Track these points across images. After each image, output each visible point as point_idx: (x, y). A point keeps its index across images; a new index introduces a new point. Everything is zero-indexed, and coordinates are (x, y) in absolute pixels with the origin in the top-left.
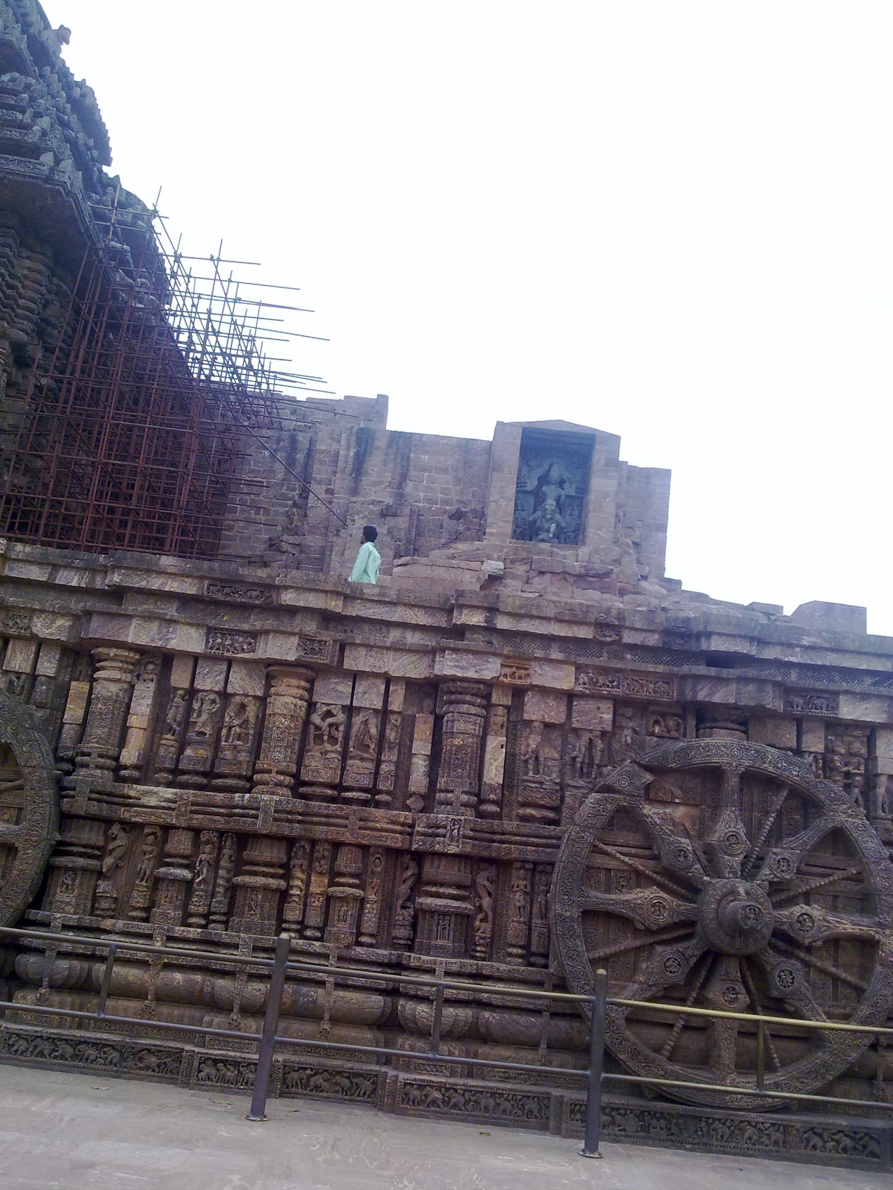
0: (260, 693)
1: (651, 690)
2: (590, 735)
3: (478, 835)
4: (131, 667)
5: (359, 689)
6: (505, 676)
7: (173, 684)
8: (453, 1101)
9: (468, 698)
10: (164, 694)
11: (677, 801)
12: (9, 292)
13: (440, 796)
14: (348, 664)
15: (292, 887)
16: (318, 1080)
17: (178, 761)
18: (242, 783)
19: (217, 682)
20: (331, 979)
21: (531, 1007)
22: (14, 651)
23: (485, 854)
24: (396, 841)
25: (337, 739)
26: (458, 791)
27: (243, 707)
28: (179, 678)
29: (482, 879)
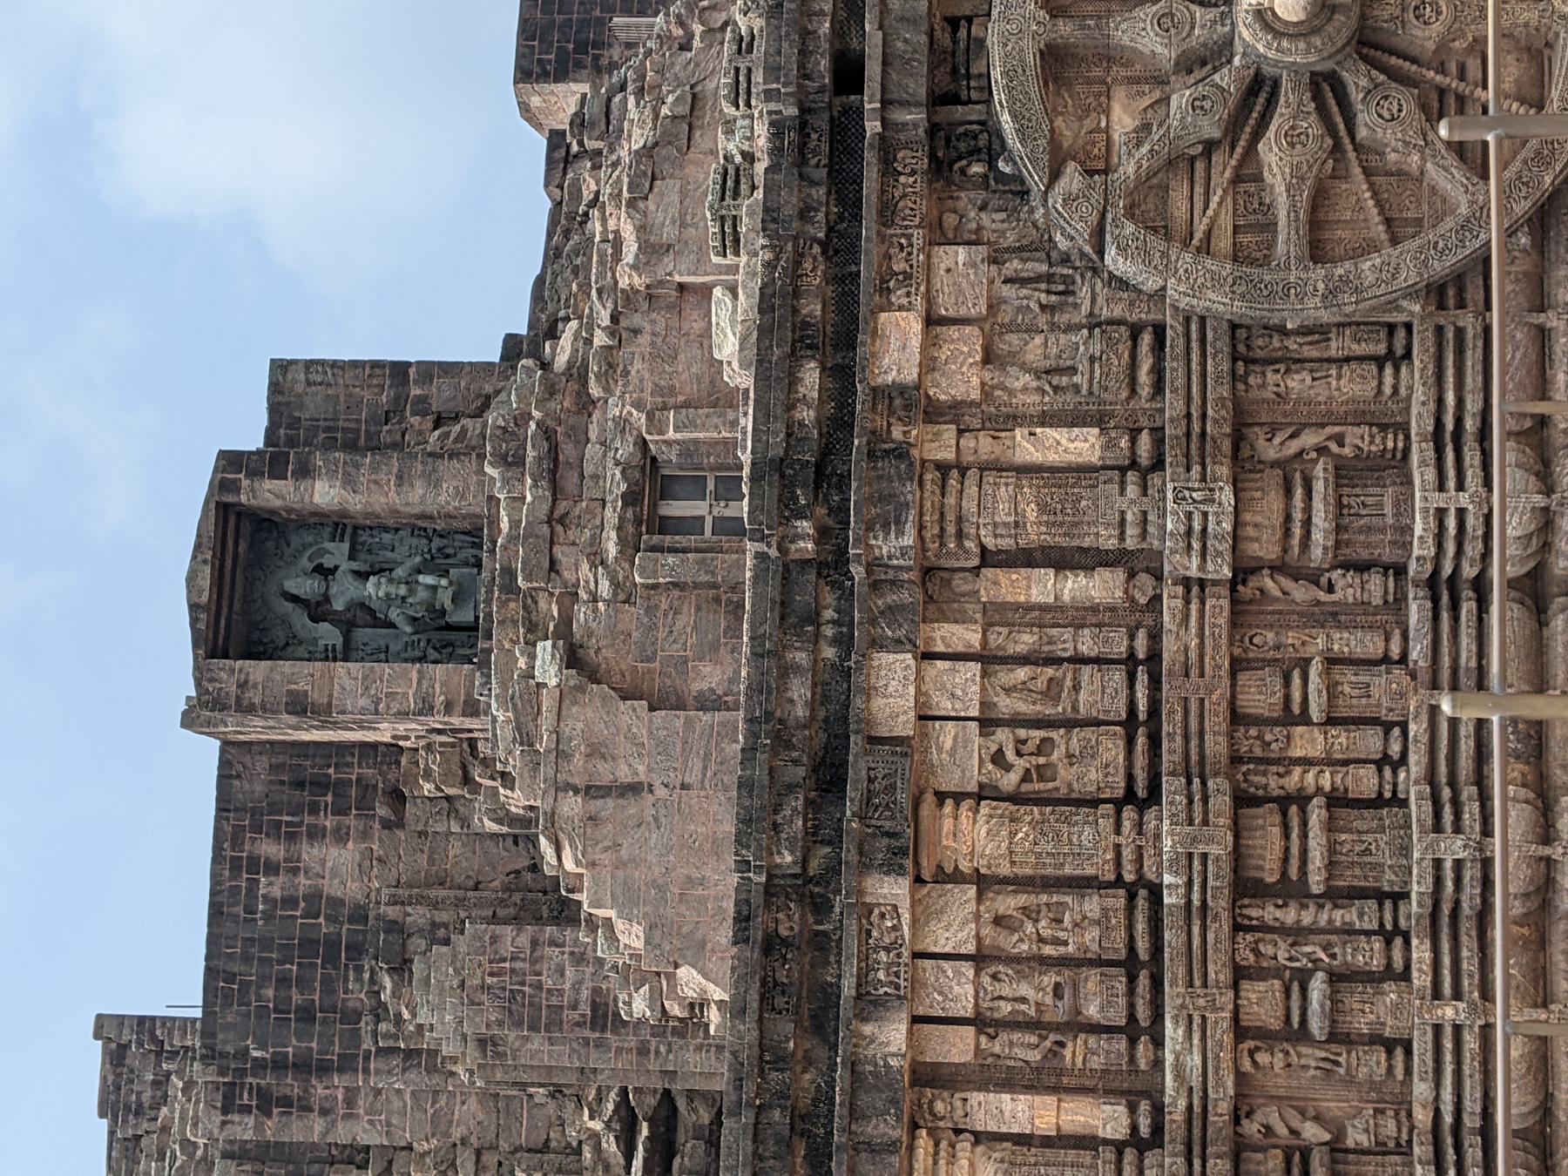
0: (972, 891)
1: (911, 180)
2: (998, 283)
4: (944, 1144)
5: (946, 706)
7: (968, 1057)
11: (1103, 124)
13: (1130, 544)
14: (904, 725)
15: (1319, 789)
17: (1110, 1030)
18: (1141, 903)
19: (958, 973)
21: (1480, 344)
23: (1226, 446)
24: (1218, 605)
25: (1043, 740)
27: (998, 921)
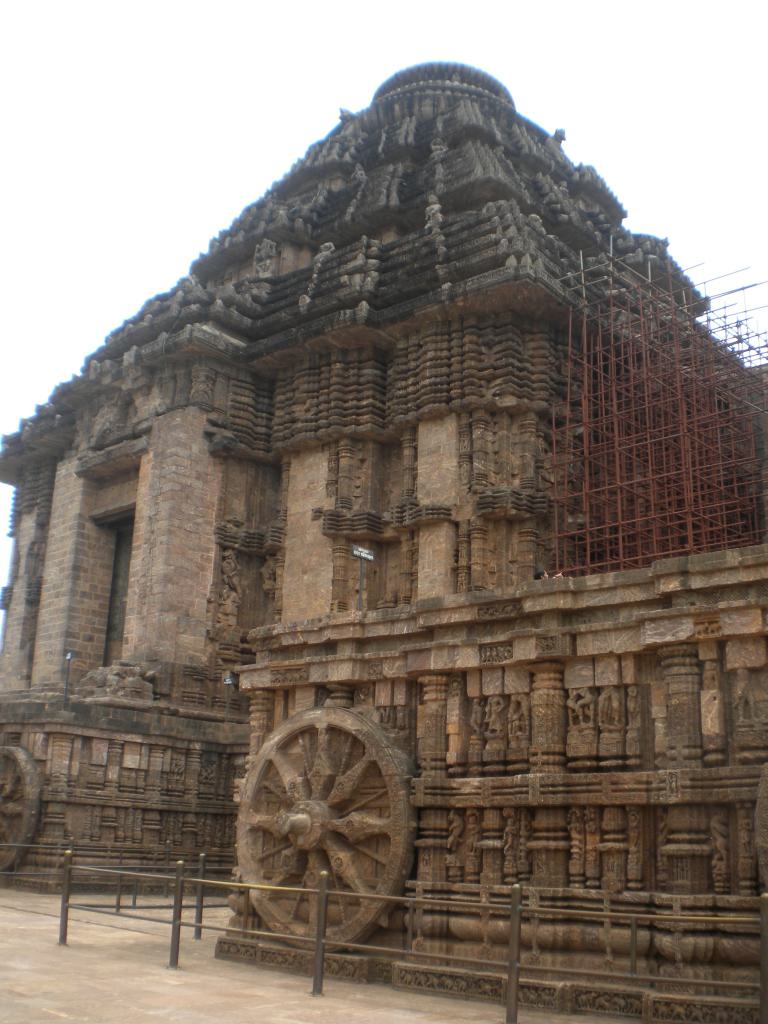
3: (700, 783)
6: (699, 633)
8: (694, 1014)
9: (676, 660)
10: (467, 702)
12: (521, 374)
14: (582, 651)
15: (571, 847)
16: (602, 1000)
20: (607, 920)
22: (379, 692)
24: (640, 798)
26: (679, 746)
27: (519, 704)
28: (473, 691)
29: (715, 824)
